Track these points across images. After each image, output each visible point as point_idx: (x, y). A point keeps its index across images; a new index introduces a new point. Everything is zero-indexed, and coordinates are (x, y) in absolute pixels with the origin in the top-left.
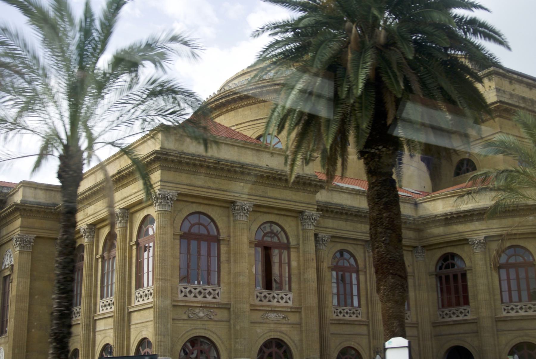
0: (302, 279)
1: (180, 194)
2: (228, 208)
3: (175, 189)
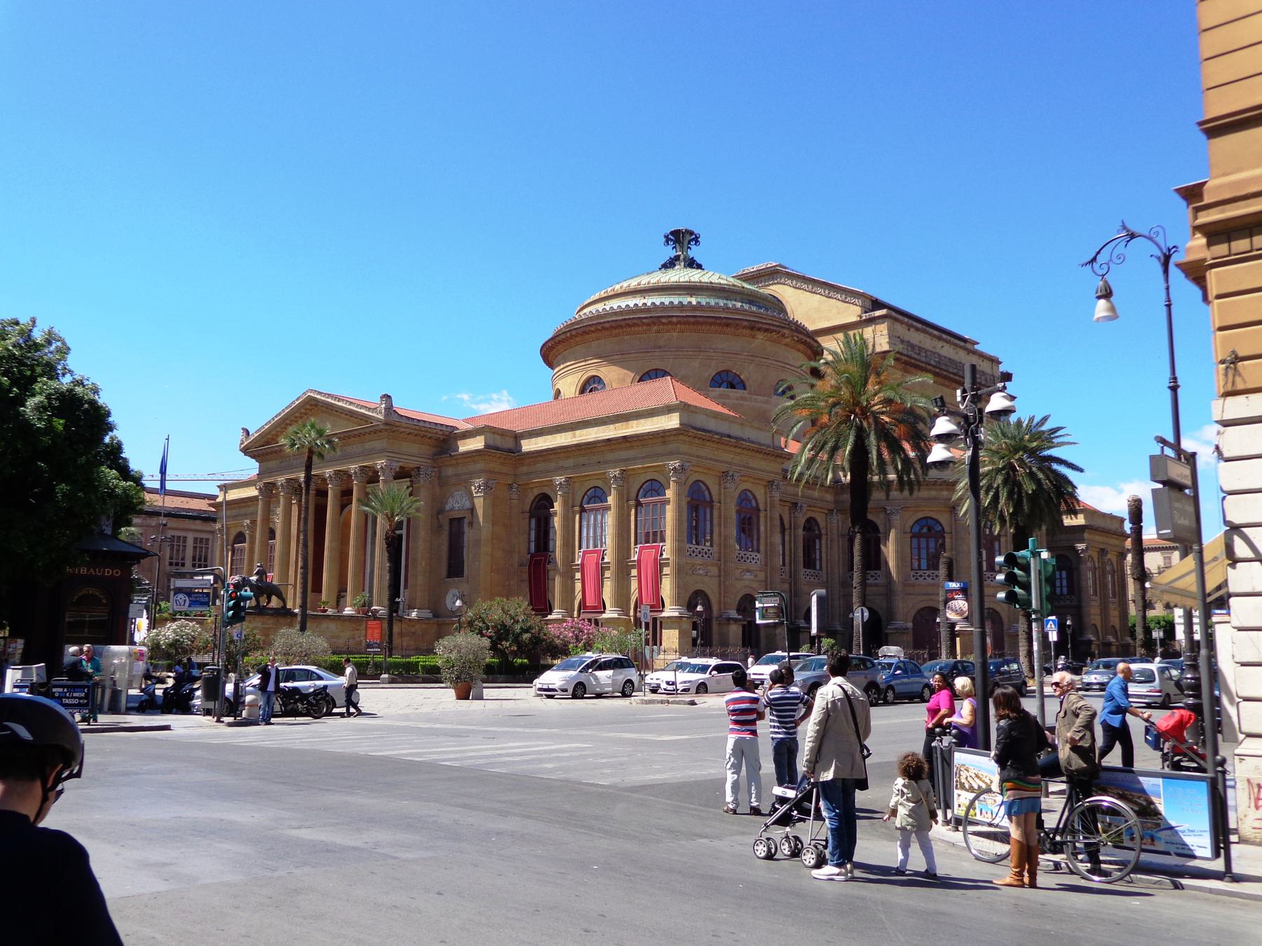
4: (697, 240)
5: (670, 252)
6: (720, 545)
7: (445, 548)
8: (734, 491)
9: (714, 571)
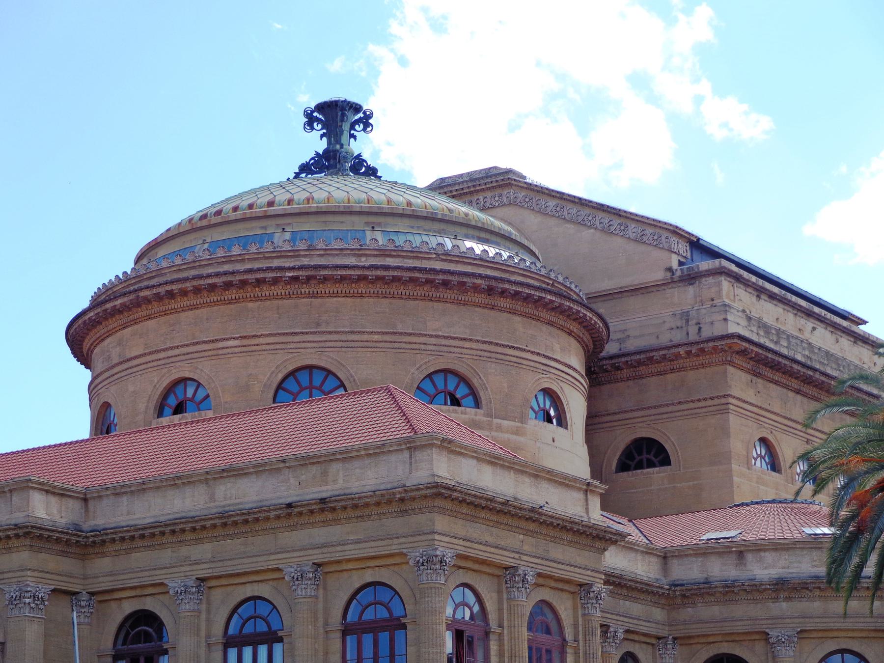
1: (459, 556)
2: (498, 576)
3: (451, 546)
4: (366, 122)
5: (315, 143)
8: (526, 602)
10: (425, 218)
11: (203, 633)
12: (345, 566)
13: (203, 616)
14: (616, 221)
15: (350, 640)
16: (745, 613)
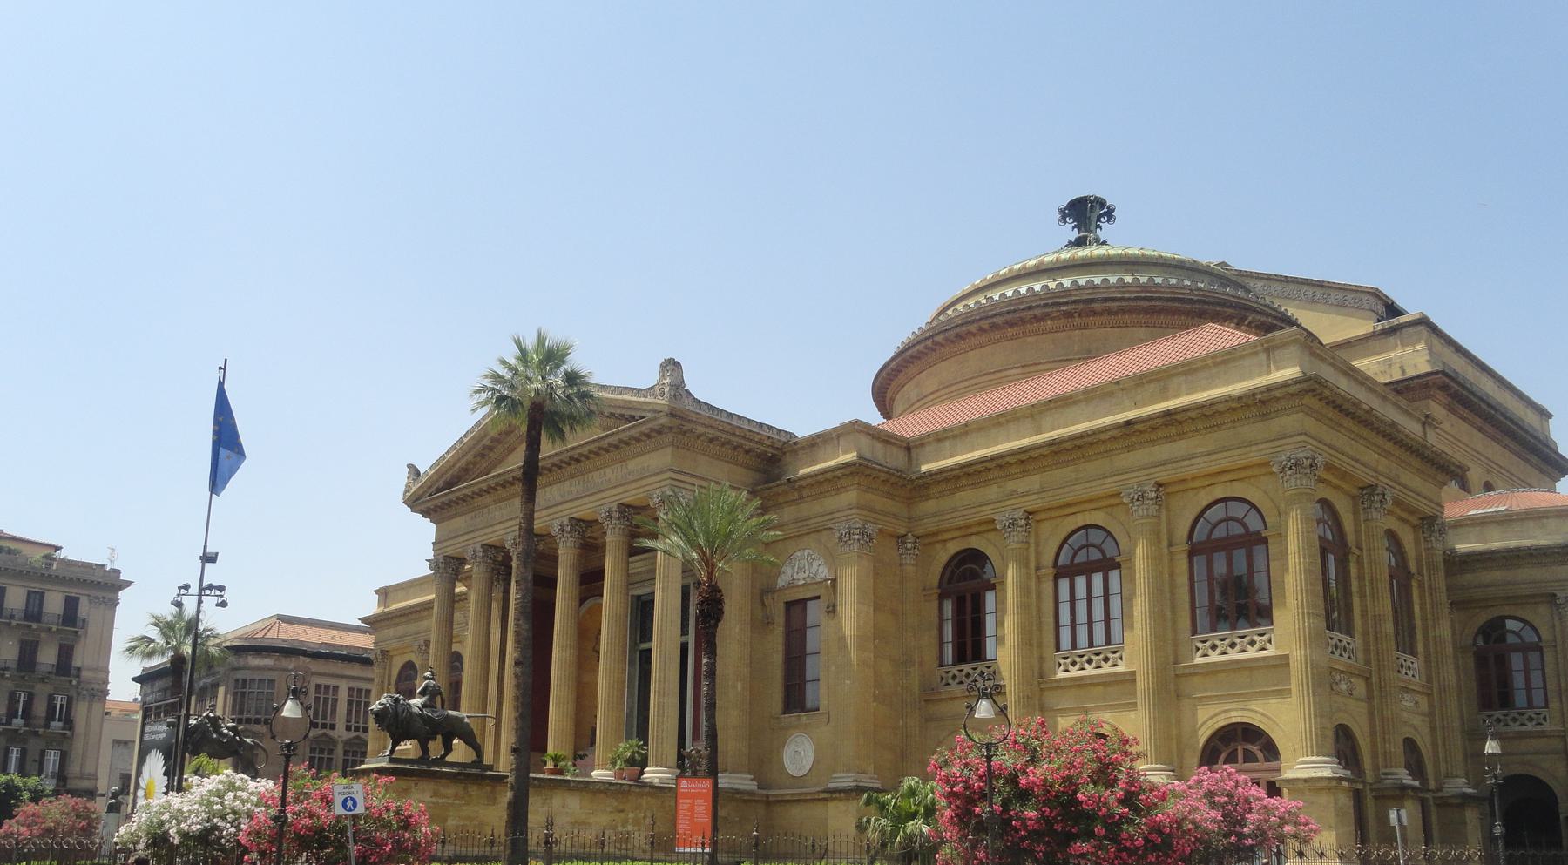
0: (1431, 634)
4: (1110, 214)
6: (1365, 634)
7: (778, 658)
9: (1360, 688)
10: (1176, 267)
11: (1033, 565)
12: (1191, 485)
13: (1032, 548)
14: (1319, 292)
15: (1200, 561)
16: (1527, 574)
